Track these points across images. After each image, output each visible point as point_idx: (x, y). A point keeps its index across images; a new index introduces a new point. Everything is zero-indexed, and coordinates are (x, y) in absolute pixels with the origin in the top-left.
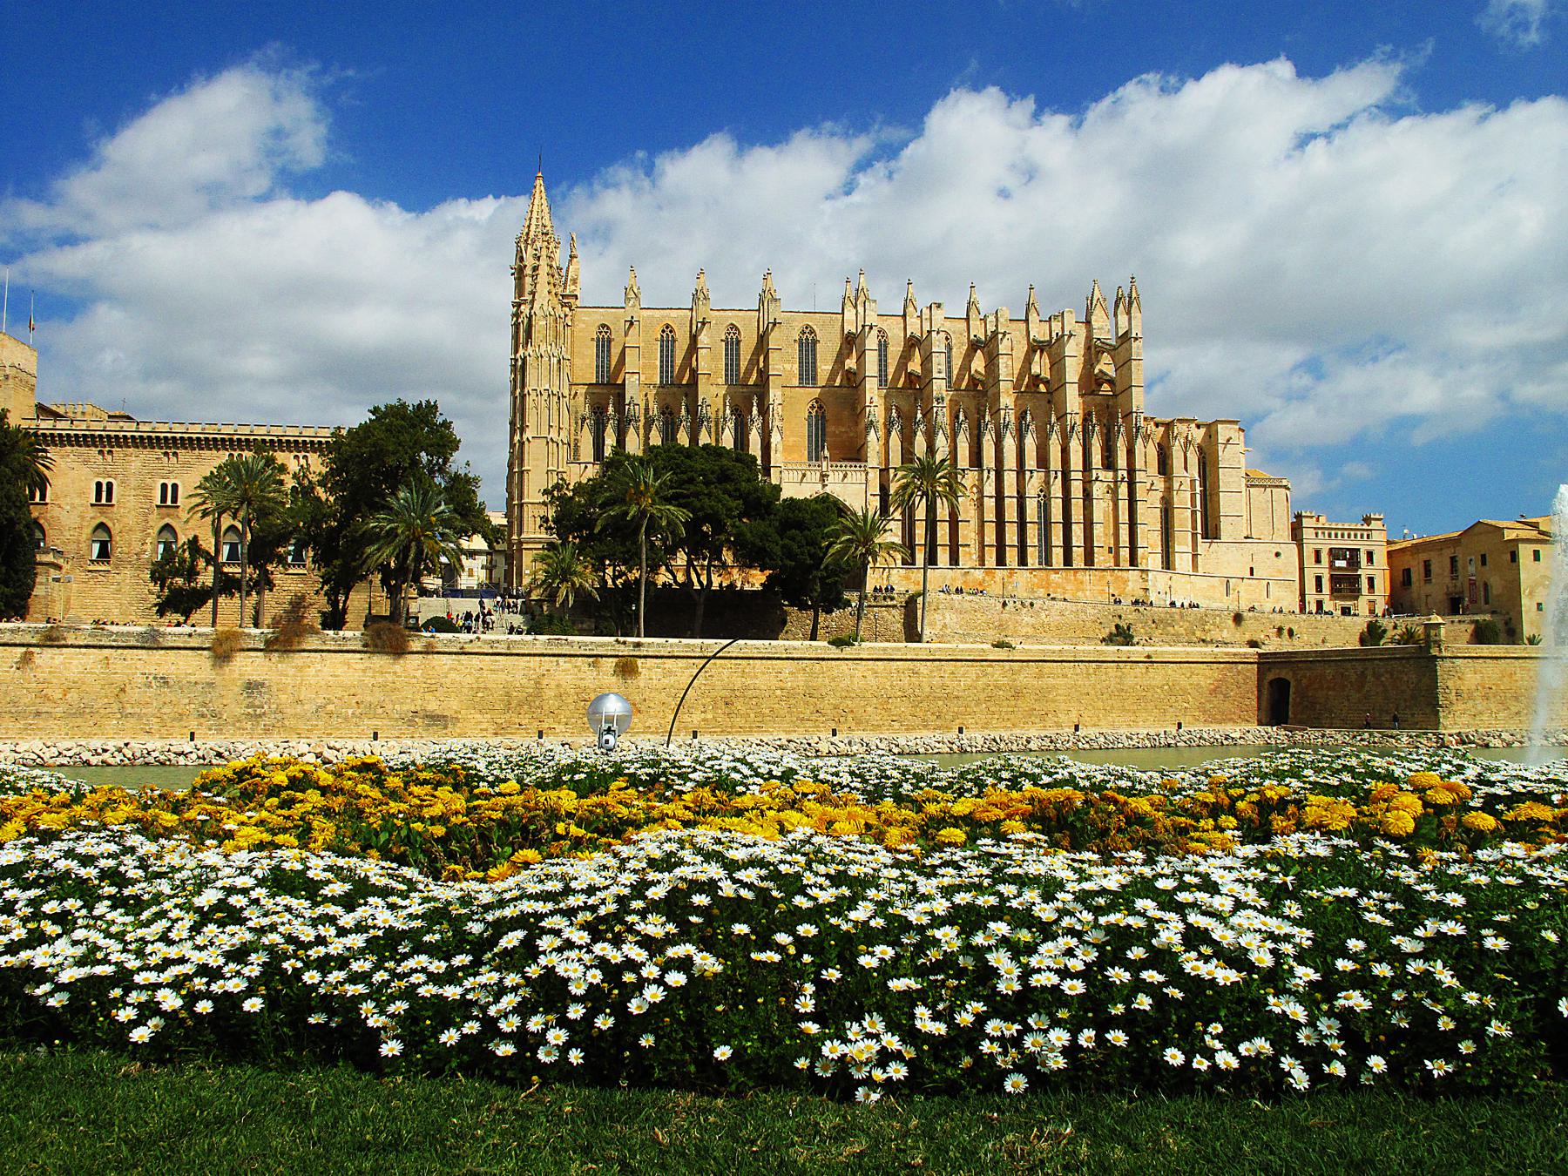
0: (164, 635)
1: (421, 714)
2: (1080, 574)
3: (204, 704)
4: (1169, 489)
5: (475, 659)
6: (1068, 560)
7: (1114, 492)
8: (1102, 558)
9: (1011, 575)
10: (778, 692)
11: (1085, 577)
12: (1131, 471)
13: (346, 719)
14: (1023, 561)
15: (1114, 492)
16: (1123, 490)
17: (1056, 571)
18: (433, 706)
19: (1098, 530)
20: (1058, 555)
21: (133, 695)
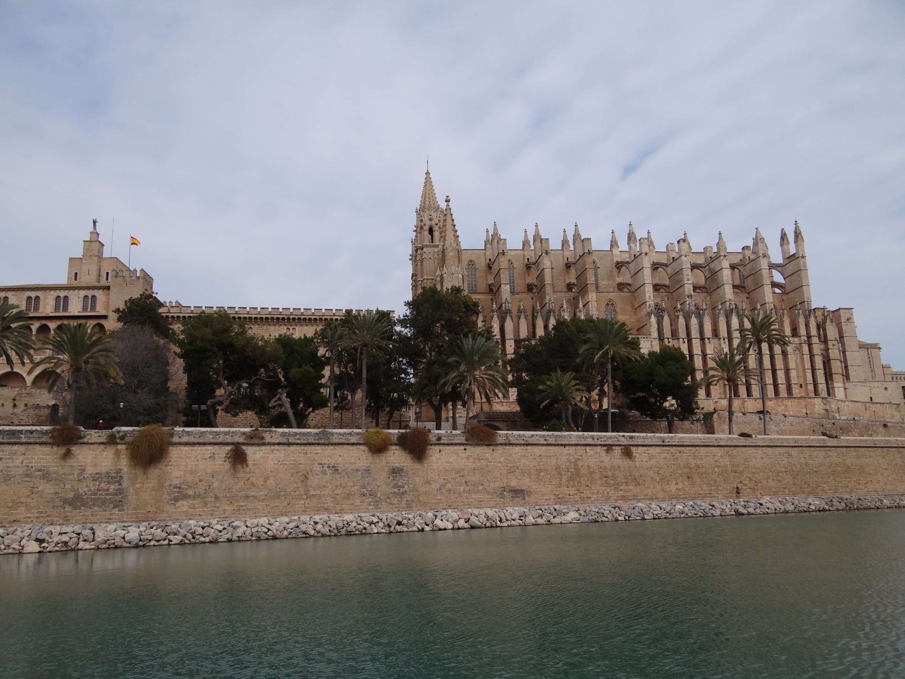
0: (333, 434)
1: (507, 489)
2: (785, 402)
3: (364, 487)
4: (827, 350)
5: (536, 449)
6: (777, 393)
7: (799, 349)
8: (796, 391)
9: (744, 402)
10: (716, 469)
11: (789, 403)
12: (809, 337)
13: (460, 494)
14: (749, 394)
15: (799, 349)
16: (805, 348)
17: (771, 399)
18: (514, 483)
19: (793, 374)
20: (770, 389)
21: (314, 481)
